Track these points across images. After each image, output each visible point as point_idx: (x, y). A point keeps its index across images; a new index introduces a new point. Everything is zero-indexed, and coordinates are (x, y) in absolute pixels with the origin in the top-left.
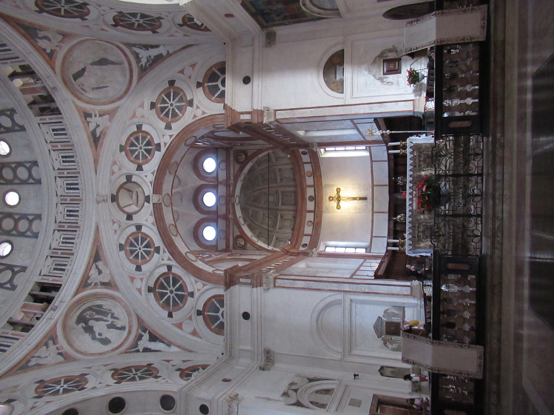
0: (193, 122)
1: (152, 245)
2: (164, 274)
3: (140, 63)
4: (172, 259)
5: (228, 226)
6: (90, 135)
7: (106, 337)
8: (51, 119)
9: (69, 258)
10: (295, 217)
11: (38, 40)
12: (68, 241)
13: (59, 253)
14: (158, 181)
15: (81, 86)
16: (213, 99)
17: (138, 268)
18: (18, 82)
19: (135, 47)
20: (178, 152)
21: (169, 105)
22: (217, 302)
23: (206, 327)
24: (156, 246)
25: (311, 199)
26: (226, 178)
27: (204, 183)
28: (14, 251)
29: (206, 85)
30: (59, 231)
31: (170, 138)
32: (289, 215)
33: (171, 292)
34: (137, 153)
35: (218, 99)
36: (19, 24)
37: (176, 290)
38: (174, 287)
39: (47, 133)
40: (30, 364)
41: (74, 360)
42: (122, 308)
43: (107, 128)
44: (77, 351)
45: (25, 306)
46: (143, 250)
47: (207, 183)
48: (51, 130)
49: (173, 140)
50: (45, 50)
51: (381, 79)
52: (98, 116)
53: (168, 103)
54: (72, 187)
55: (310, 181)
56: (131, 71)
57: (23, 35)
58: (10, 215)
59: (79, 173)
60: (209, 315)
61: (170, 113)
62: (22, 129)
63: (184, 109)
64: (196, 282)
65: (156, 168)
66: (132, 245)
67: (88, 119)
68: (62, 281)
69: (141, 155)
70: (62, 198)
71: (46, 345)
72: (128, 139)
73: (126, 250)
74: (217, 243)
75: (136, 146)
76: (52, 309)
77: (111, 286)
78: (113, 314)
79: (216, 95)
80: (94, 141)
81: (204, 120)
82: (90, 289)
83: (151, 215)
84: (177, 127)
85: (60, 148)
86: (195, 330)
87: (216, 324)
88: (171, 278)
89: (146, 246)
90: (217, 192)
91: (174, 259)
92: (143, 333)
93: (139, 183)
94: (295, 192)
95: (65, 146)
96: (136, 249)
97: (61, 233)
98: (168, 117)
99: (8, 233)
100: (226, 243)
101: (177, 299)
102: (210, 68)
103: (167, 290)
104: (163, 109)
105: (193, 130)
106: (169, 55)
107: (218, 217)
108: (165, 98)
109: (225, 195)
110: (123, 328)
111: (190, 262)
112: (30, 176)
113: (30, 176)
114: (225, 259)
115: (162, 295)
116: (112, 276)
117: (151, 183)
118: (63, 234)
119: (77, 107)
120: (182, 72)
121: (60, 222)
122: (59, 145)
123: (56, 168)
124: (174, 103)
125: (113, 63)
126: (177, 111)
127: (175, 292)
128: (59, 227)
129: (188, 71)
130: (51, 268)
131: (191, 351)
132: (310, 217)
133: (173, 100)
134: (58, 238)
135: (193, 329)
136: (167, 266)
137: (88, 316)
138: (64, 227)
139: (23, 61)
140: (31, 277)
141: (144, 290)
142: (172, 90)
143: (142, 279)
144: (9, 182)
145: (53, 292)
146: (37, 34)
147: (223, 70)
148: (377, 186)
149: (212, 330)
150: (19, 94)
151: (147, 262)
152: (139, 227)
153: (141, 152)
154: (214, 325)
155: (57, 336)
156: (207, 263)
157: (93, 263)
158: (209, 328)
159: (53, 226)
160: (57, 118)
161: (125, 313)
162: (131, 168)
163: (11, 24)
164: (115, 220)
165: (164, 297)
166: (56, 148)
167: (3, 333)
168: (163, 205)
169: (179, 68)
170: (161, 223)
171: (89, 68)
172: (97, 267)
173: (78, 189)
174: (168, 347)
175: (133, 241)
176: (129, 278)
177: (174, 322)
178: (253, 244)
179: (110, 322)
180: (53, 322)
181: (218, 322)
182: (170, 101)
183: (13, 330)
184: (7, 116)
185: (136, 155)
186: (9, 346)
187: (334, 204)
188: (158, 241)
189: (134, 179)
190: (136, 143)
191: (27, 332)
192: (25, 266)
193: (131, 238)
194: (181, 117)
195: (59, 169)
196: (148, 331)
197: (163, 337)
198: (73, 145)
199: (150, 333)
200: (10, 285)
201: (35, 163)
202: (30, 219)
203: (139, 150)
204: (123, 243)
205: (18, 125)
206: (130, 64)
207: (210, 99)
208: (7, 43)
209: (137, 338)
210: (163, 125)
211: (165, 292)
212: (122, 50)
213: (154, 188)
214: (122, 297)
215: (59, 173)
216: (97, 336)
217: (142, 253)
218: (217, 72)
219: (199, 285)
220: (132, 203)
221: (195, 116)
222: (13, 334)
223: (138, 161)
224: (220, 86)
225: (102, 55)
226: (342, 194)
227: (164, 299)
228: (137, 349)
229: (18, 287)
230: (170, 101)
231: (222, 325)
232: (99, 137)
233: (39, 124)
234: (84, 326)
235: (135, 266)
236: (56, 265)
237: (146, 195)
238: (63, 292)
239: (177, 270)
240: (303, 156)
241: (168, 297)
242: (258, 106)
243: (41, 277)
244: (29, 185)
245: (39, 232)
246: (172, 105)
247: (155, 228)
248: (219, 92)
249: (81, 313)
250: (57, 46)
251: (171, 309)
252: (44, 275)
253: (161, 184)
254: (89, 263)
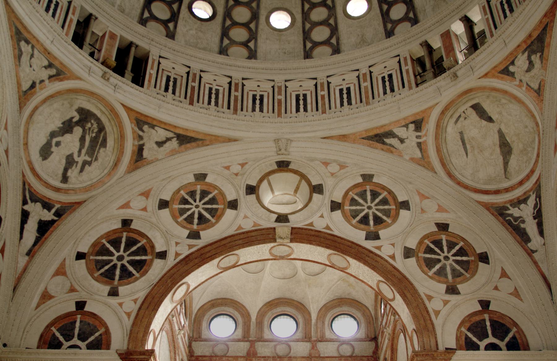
0: (419, 295)
1: (203, 226)
2: (153, 247)
3: (511, 205)
4: (178, 260)
6: (387, 129)
7: (52, 152)
8: (407, 71)
9: (186, 98)
11: (526, 54)
12: (213, 96)
13: (193, 84)
14: (313, 236)
15: (463, 115)
16: (463, 329)
17: (163, 204)
18: (458, 28)
19: (536, 197)
20: (366, 269)
21: (446, 254)
22: (96, 338)
23: (54, 316)
24: (201, 233)
26: (322, 355)
27: (314, 316)
28: (199, 22)
29: (486, 316)
30: (230, 83)
31: (390, 257)
33: (120, 258)
34: (361, 201)
35: (463, 338)
36: (545, 29)
37: (123, 266)
38: (128, 262)
39: (385, 67)
40: (23, 43)
41: (22, 105)
42: (99, 177)
43: (401, 156)
44: (36, 108)
45: (113, 36)
46: (193, 214)
47: (313, 321)
48: (390, 73)
49: (387, 261)
50: (513, 63)
52: (419, 140)
53: (448, 252)
54: (301, 102)
56: (497, 192)
57: (530, 36)
58: (255, 16)
59: (324, 112)
60: (75, 322)
61: (433, 256)
62: (389, 34)
63: (442, 279)
64: (135, 301)
65: (336, 233)
66: (204, 194)
67: (412, 127)
68: (148, 88)
69: (358, 208)
70: (283, 88)
71: (50, 66)
72: (384, 188)
73: (196, 185)
74: (206, 340)
75: (373, 200)
76: (105, 73)
77: (137, 161)
78: (90, 163)
79: (470, 335)
80: (376, 136)
81: (425, 314)
82: (133, 129)
83: (255, 224)
85: (363, 85)
86: (51, 297)
87: (58, 334)
88: (144, 258)
89: (201, 216)
90: (298, 341)
91: (178, 263)
92: (53, 211)
93: (310, 205)
95: (367, 92)
96: (198, 200)
97: (227, 86)
98: (425, 252)
99: (228, 14)
100: (205, 356)
101: (107, 267)
102: (516, 325)
103: (125, 251)
104: (438, 243)
105: (405, 296)
106: (530, 253)
107: (252, 343)
108: (457, 248)
109: (292, 354)
110: (65, 179)
111: (171, 290)
112: (316, 44)
113: (316, 44)
114: (175, 353)
115: (116, 243)
116: (152, 162)
117: (311, 224)
118: (224, 89)
119: (431, 108)
120: (504, 274)
121: (243, 85)
122: (368, 84)
123: (330, 80)
124: (450, 261)
125: (506, 164)
126: (437, 267)
127: (119, 264)
128: (237, 85)
129: (506, 286)
130: (170, 72)
131: (15, 289)
133: (457, 262)
134: (218, 82)
135: (53, 295)
136: (166, 251)
137: (89, 125)
138: (236, 90)
139: (492, 35)
140: (158, 45)
141: (126, 214)
142: (473, 258)
143: (145, 209)
144: (306, 16)
145: (133, 75)
146: (534, 52)
147: (513, 346)
149: (49, 327)
150: (443, 30)
151: (174, 217)
152: (233, 205)
153: (363, 208)
154: (58, 330)
155: (61, 80)
156: (169, 320)
157: (175, 133)
158: (52, 324)
159: (237, 76)
160: (409, 82)
161: (89, 183)
163: (544, 20)
164: (247, 167)
165: (111, 245)
166: (361, 80)
167: (75, 8)
168: (272, 245)
169: (509, 270)
170: (240, 242)
171: (493, 128)
172: (168, 139)
173: (298, 110)
174: (26, 251)
175: (210, 196)
176: (148, 189)
177: (67, 262)
179: (76, 160)
180: (84, 74)
181: (61, 339)
182: (454, 255)
183: (78, 21)
184: (407, 13)
185: (356, 201)
186: (54, 15)
189: (315, 195)
190: (377, 200)
191: (73, 40)
192: (176, 38)
193: (216, 192)
194: (426, 274)
195: (329, 83)
196: (56, 218)
197: (44, 242)
198: (368, 103)
199: (53, 222)
200: (147, 18)
201: (337, 51)
202: (249, 44)
203: (366, 205)
204: (208, 180)
205: (394, 28)
206: (507, 190)
207: (462, 324)
208: (515, 14)
209: (47, 201)
210: (412, 244)
211: (120, 247)
212: (528, 177)
213: (302, 229)
214: (115, 178)
215: (322, 84)
216: (55, 140)
217: (189, 209)
218: (510, 335)
219: (132, 307)
220: (276, 193)
221: (430, 298)
222: (71, 20)
223: (348, 205)
224: (486, 342)
225: (517, 147)
227: (108, 246)
228: (29, 201)
229: (144, 27)
230: (454, 255)
231: (55, 345)
232: (384, 143)
233: (399, 56)
234: (75, 120)
235: (168, 199)
236: (175, 80)
237: (289, 217)
238: (132, 90)
241: (112, 253)
243: (157, 58)
244: (302, 42)
245: (227, 55)
246: (446, 258)
247: (231, 232)
248: (475, 339)
249: (94, 115)
250: (521, 81)
251: (92, 257)
252: (159, 63)
253: (309, 242)
254: (175, 127)
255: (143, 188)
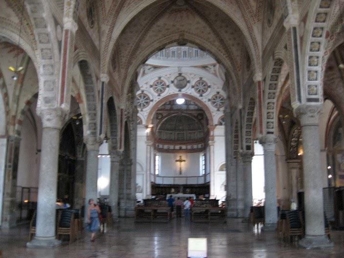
5: (167, 110)
10: (171, 140)
17: (151, 86)
25: (181, 149)
32: (173, 137)
43: (209, 72)
51: (223, 184)
55: (189, 147)
65: (192, 95)
84: (209, 104)
94: (183, 140)
104: (216, 97)
124: (218, 102)
132: (172, 147)
133: (221, 102)
148: (187, 179)
151: (154, 90)
152: (168, 86)
162: (193, 83)
178: (159, 123)
187: (178, 159)
188: (164, 95)
204: (162, 79)
210: (210, 97)
226: (183, 163)
239: (152, 104)
240: (200, 145)
242: (216, 139)
247: (168, 95)
255: (145, 82)
